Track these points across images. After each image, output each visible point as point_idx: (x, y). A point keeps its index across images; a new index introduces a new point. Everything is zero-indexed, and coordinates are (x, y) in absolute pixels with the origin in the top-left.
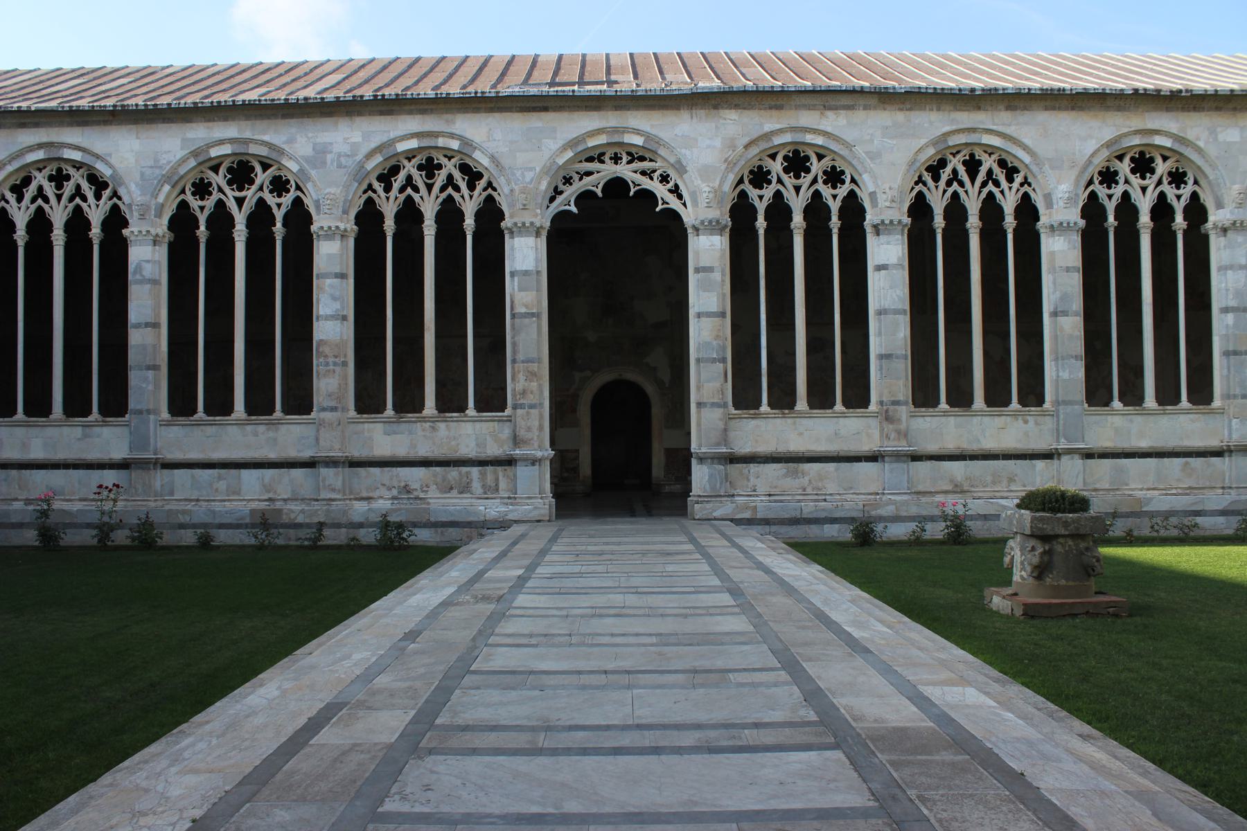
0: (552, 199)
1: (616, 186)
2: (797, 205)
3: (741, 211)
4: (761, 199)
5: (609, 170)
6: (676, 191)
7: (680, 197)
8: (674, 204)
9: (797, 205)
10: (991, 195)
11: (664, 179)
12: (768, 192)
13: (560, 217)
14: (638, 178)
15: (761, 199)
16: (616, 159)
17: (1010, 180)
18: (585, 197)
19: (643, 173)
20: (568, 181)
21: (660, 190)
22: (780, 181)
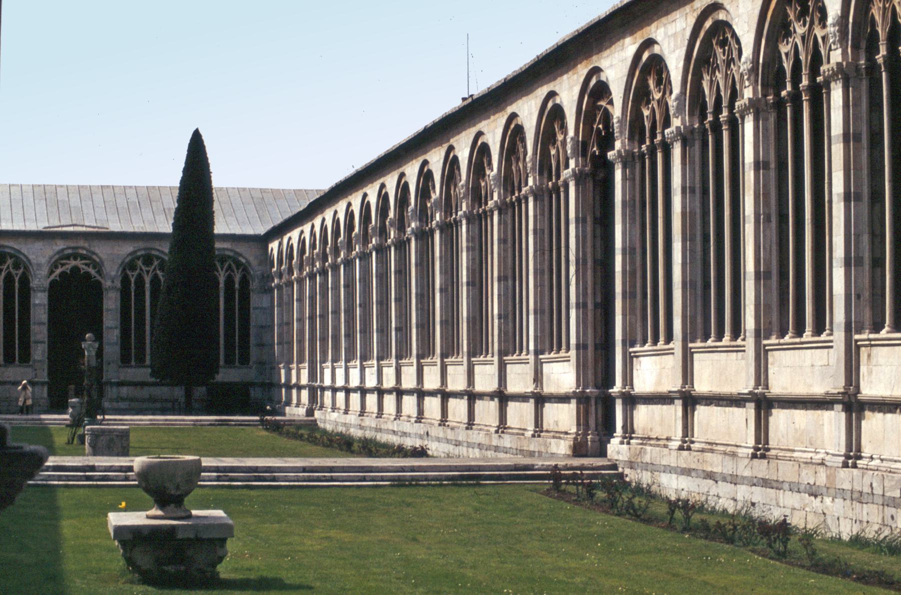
0: (50, 274)
1: (75, 269)
2: (147, 279)
3: (125, 280)
4: (133, 277)
5: (73, 263)
6: (99, 272)
7: (100, 275)
8: (99, 278)
9: (147, 279)
10: (230, 275)
11: (94, 268)
12: (136, 273)
13: (53, 284)
14: (84, 267)
15: (133, 277)
16: (75, 259)
17: (238, 269)
18: (62, 274)
19: (86, 264)
20: (56, 267)
21: (93, 272)
22: (141, 269)
